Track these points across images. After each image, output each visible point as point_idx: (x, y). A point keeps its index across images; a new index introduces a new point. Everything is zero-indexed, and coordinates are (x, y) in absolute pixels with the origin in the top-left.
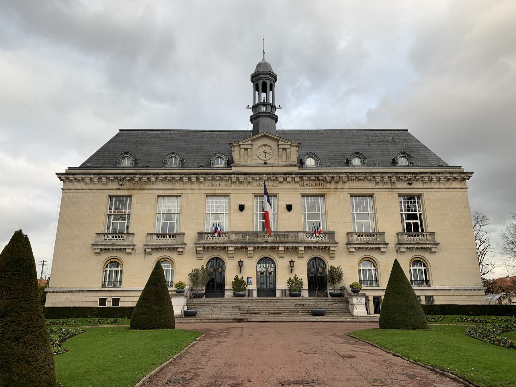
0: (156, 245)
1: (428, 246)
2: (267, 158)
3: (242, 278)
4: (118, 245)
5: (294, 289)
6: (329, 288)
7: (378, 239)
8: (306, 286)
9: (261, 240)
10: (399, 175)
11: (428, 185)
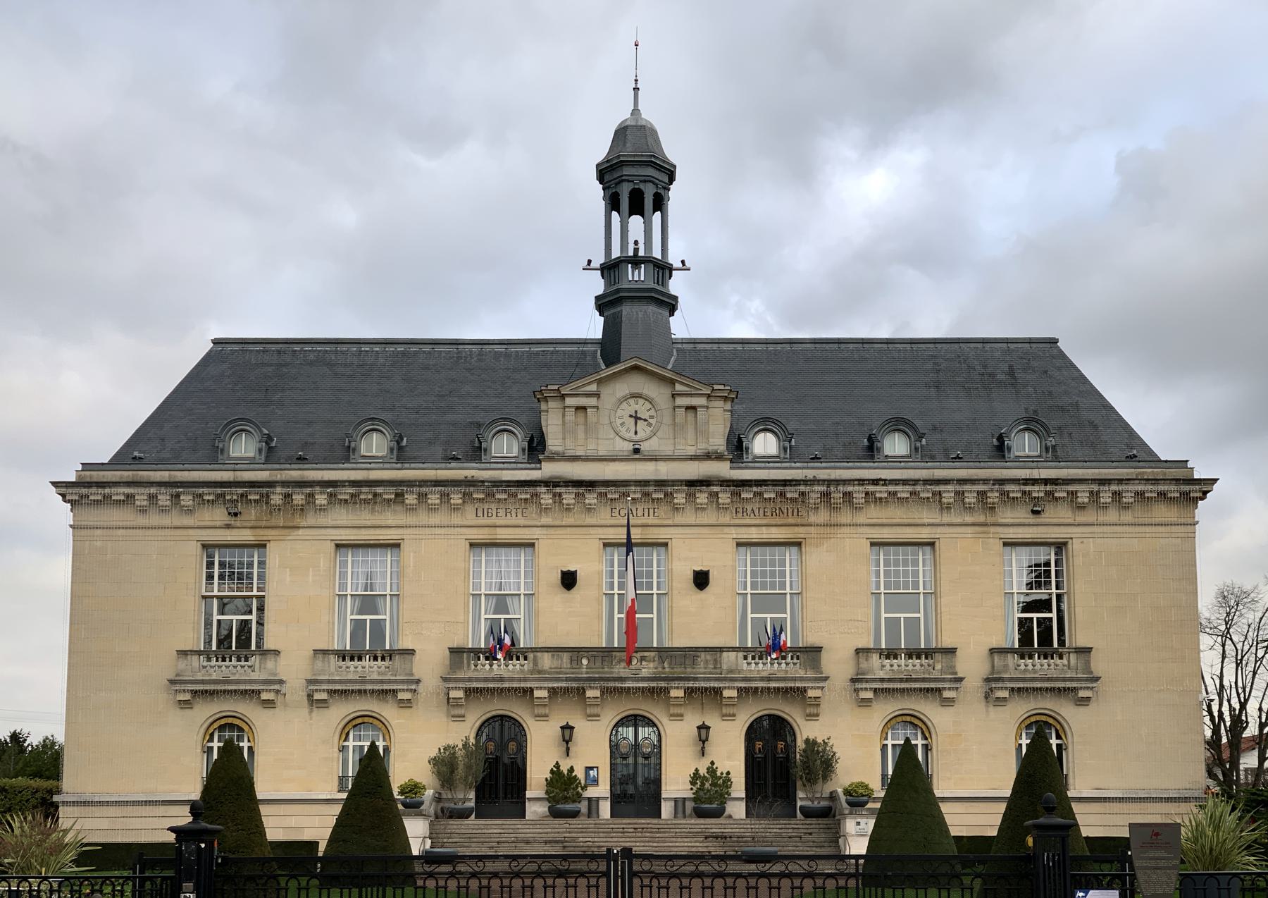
0: (340, 682)
1: (1069, 685)
2: (641, 435)
3: (571, 770)
4: (238, 682)
5: (708, 796)
6: (800, 794)
7: (938, 667)
8: (739, 788)
9: (620, 670)
10: (1008, 488)
11: (1089, 516)
